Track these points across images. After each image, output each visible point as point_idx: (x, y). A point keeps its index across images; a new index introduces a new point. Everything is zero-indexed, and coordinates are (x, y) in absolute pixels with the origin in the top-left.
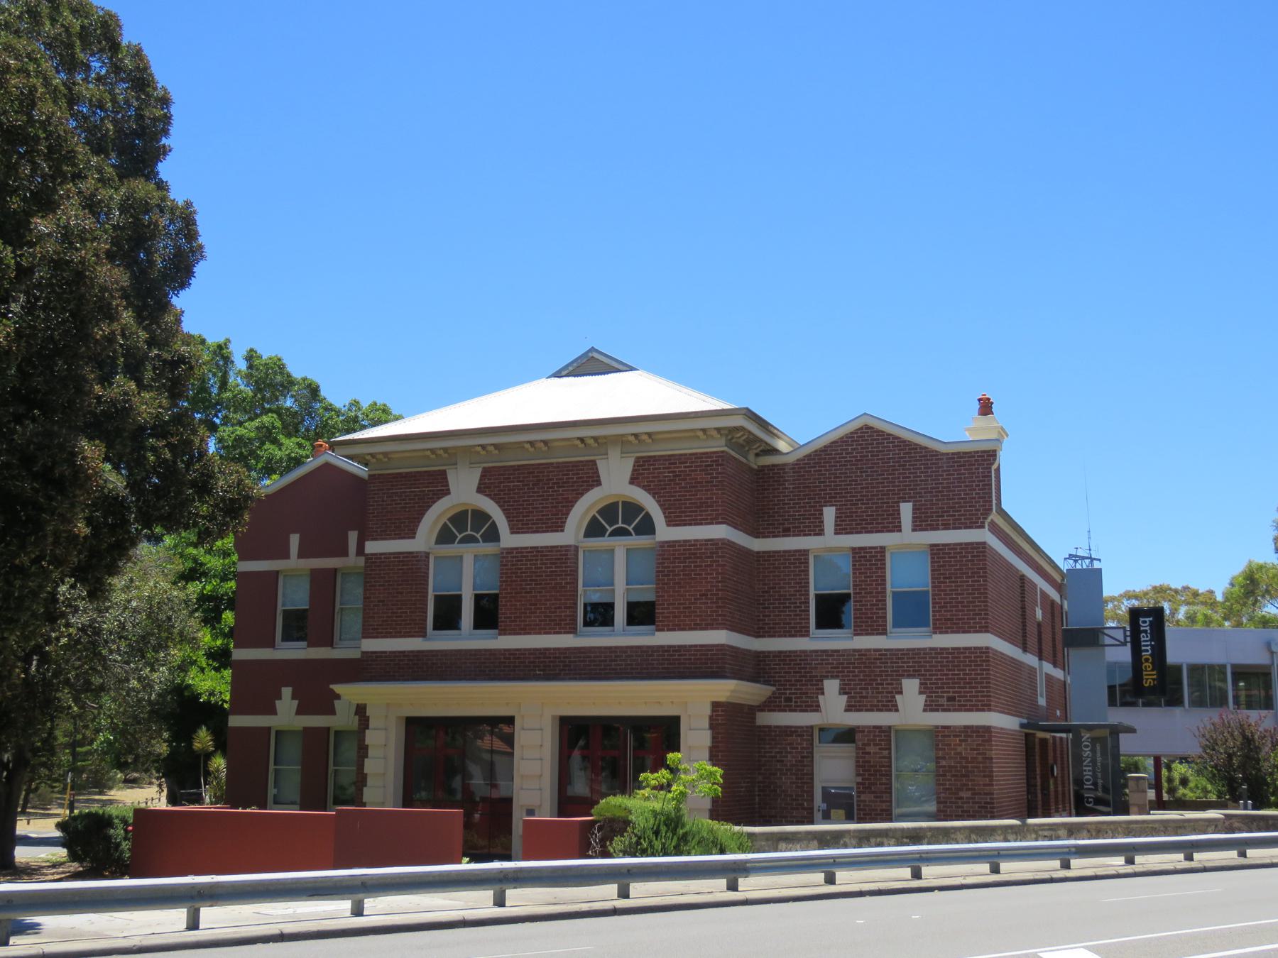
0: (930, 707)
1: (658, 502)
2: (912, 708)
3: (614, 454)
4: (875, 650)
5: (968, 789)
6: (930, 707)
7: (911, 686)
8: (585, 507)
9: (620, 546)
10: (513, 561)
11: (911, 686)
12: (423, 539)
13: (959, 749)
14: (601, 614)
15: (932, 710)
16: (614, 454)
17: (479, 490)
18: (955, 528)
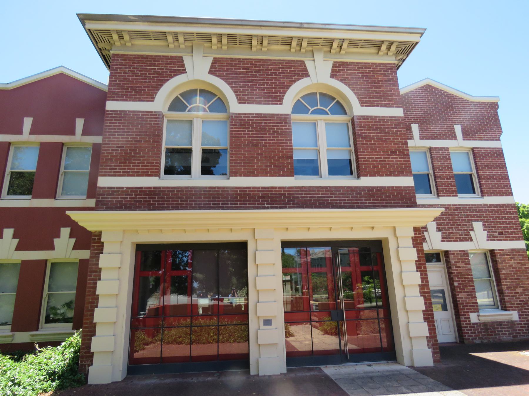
0: (491, 238)
1: (353, 90)
2: (480, 240)
3: (319, 57)
4: (454, 205)
5: (521, 287)
6: (491, 238)
7: (478, 226)
8: (295, 92)
9: (321, 120)
10: (240, 126)
11: (478, 226)
12: (160, 102)
13: (511, 263)
14: (311, 168)
15: (491, 240)
16: (319, 57)
17: (211, 72)
18: (485, 140)
